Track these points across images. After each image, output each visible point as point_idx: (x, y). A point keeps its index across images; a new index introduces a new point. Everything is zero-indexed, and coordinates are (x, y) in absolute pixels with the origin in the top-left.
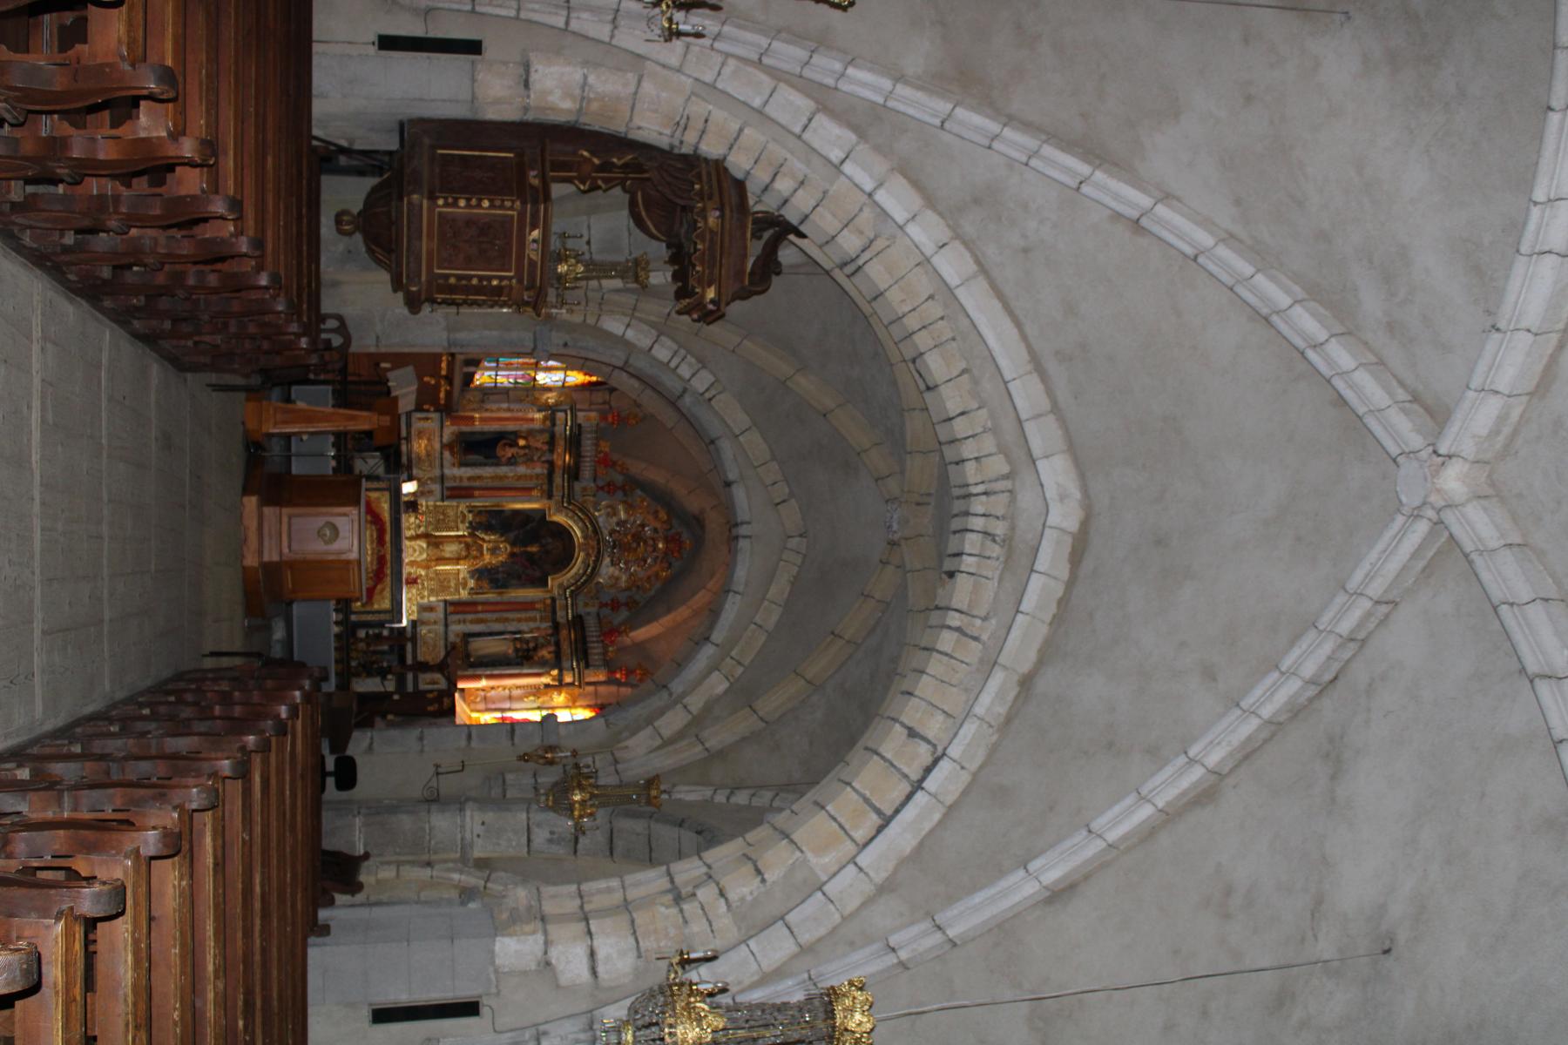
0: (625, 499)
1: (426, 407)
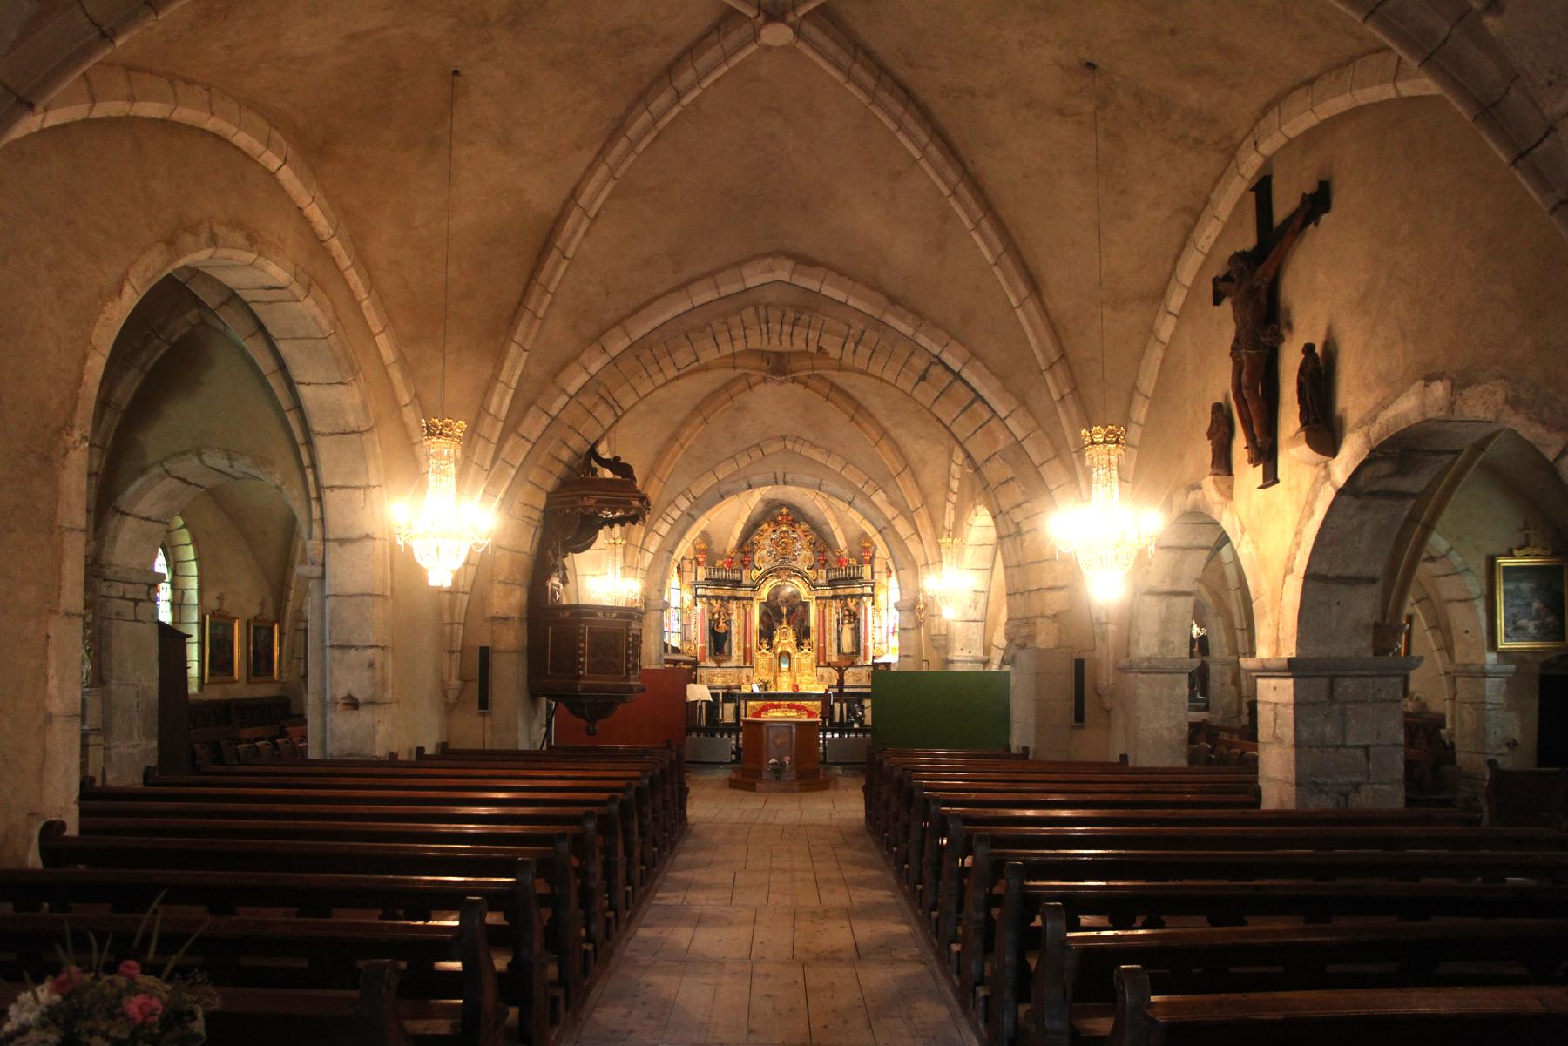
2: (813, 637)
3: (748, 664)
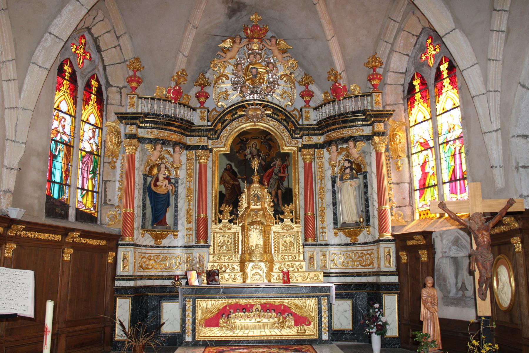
0: (212, 85)
1: (110, 260)
2: (299, 201)
3: (202, 243)
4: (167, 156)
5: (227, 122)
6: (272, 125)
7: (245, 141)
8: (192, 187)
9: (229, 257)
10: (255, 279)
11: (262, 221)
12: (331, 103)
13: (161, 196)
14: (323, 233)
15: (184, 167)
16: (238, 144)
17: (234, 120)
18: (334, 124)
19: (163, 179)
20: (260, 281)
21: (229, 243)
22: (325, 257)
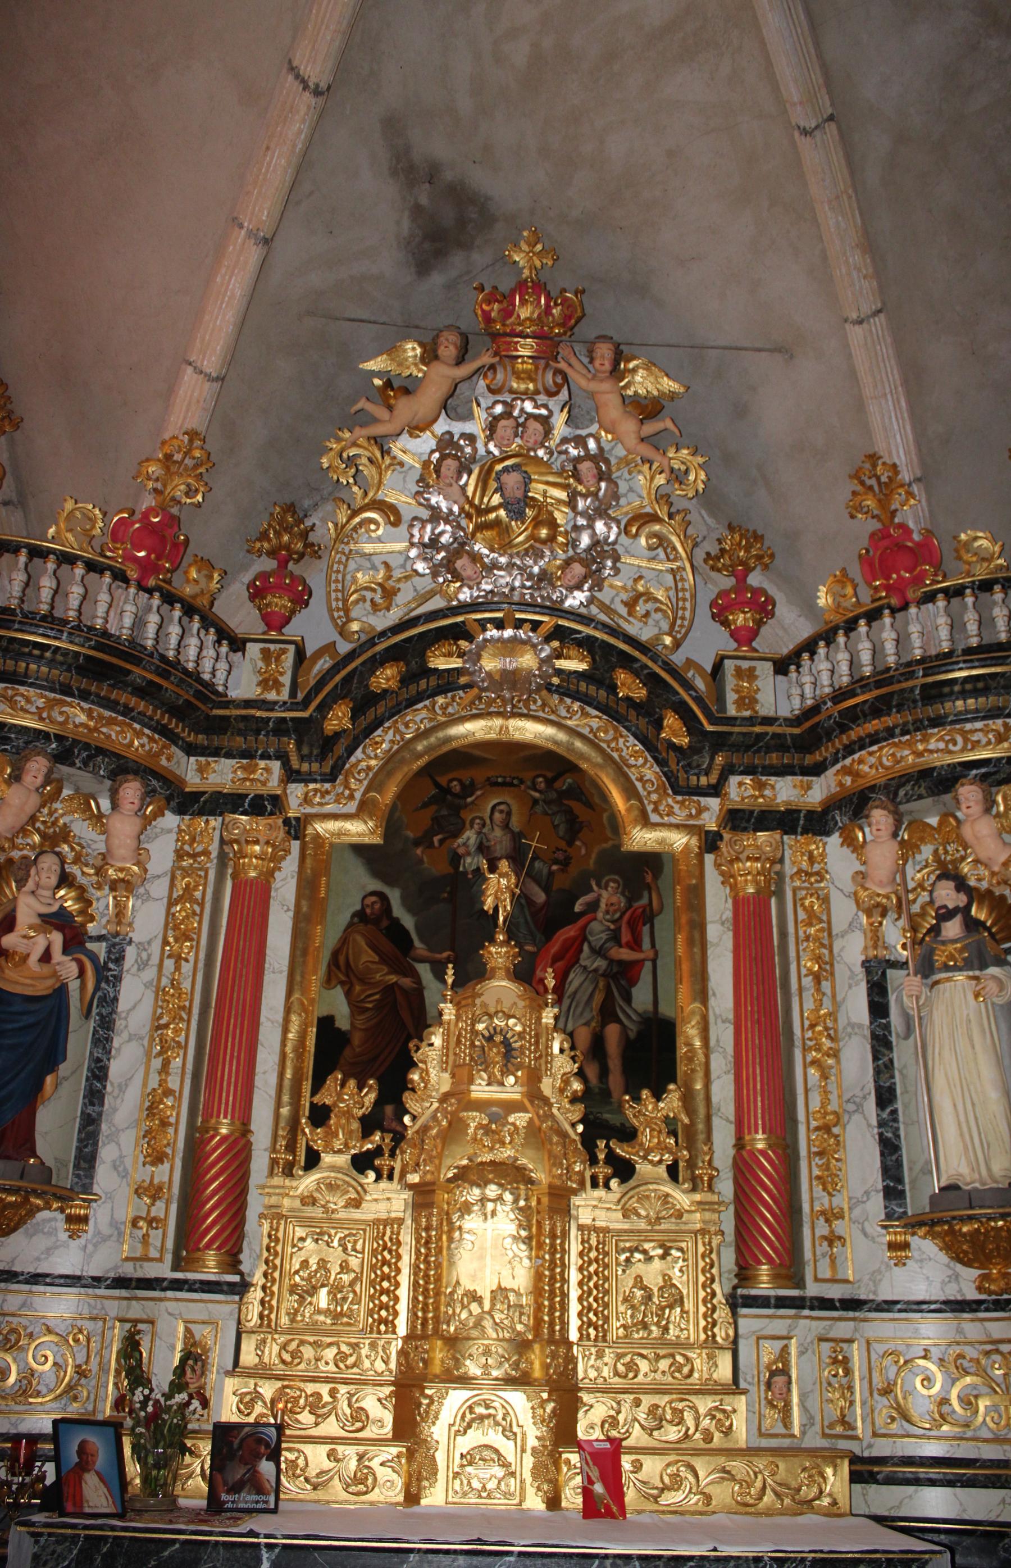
3: (210, 1269)
4: (82, 828)
5: (381, 709)
6: (586, 731)
7: (456, 795)
8: (186, 986)
9: (344, 1348)
10: (476, 1484)
11: (523, 1161)
12: (862, 622)
13: (16, 1008)
14: (831, 1245)
15: (159, 889)
16: (425, 805)
17: (411, 703)
18: (877, 709)
19: (37, 921)
20: (499, 1503)
21: (346, 1278)
22: (848, 1372)
